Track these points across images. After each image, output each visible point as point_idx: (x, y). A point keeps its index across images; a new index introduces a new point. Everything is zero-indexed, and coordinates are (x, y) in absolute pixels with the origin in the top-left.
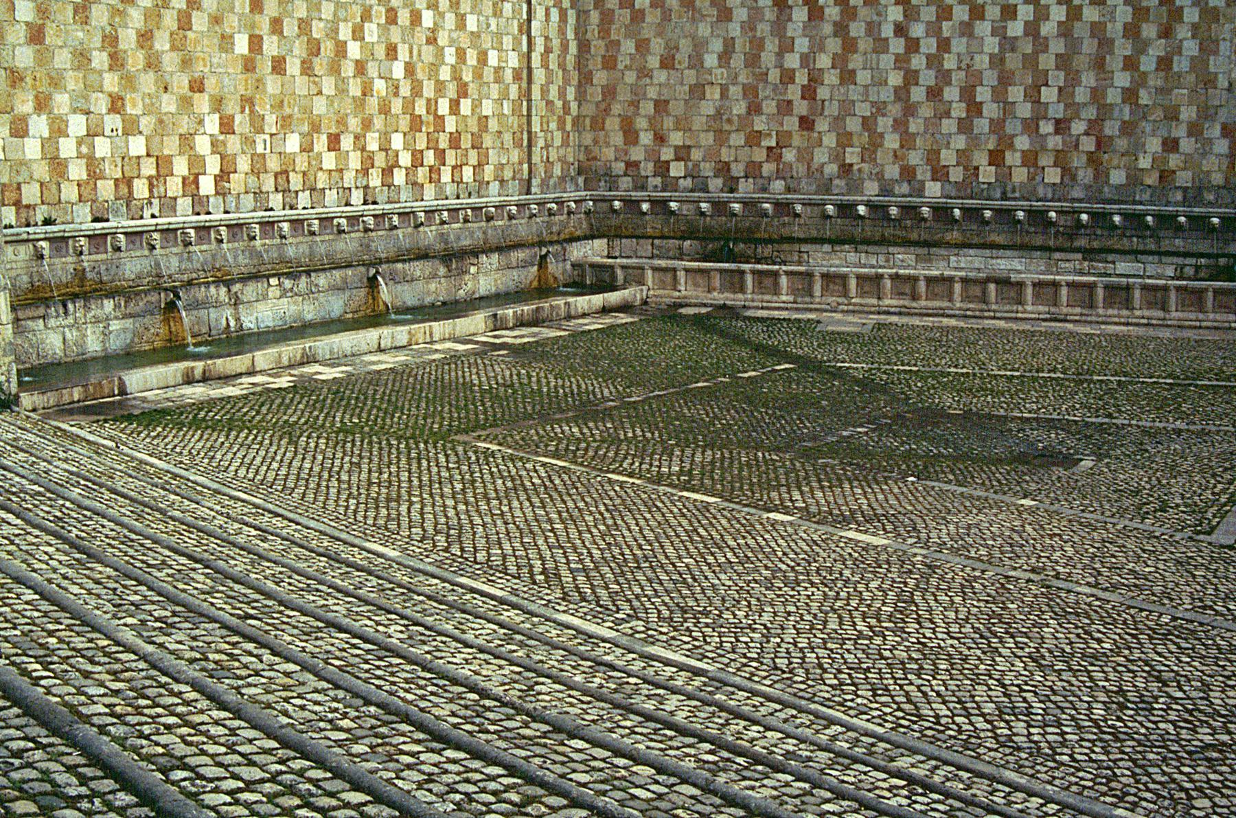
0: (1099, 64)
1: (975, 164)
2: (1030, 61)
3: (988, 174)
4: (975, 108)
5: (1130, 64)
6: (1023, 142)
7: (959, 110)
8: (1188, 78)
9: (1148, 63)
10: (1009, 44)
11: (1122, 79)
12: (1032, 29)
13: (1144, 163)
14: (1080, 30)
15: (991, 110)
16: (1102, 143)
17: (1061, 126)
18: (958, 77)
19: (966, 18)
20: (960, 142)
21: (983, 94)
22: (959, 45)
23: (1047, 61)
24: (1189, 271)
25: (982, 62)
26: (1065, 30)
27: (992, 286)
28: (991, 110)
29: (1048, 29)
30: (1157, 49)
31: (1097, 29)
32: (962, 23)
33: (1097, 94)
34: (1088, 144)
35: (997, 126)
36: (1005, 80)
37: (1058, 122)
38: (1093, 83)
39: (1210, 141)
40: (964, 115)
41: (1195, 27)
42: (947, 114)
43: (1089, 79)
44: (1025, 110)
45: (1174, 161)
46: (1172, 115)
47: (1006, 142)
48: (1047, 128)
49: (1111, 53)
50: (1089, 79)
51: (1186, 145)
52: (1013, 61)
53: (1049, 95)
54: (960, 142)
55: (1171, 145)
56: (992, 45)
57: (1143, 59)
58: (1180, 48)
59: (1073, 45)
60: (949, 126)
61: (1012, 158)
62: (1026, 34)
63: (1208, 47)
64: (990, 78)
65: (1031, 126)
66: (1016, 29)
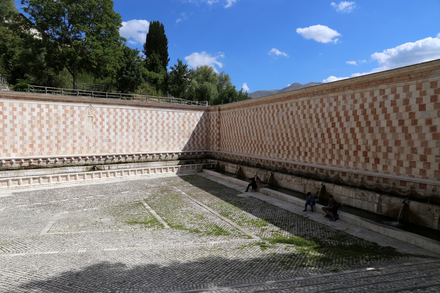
0: (57, 123)
1: (25, 148)
2: (39, 122)
3: (29, 150)
4: (25, 134)
5: (64, 123)
6: (38, 142)
7: (20, 134)
8: (78, 126)
9: (68, 123)
10: (33, 118)
11: (63, 126)
12: (39, 114)
13: (69, 145)
14: (52, 115)
15: (29, 134)
16: (59, 141)
17: (48, 138)
18: (19, 126)
19: (21, 111)
20: (21, 142)
21: (27, 130)
22: (19, 117)
23: (43, 122)
24: (85, 170)
25: (26, 122)
26: (48, 115)
27: (41, 179)
28: (29, 134)
29: (43, 114)
30: (71, 119)
31: (56, 115)
32: (20, 112)
33: (57, 130)
34: (55, 142)
35: (31, 138)
36: (33, 126)
37: (47, 137)
38: (56, 127)
39: (83, 140)
40: (21, 136)
41: (79, 115)
42: (16, 135)
43: (54, 126)
44: (38, 134)
45: (76, 145)
46: (75, 134)
47: (34, 142)
48: (44, 138)
49: (60, 120)
50: (54, 126)
51: (79, 141)
52: (35, 122)
53: (44, 130)
54: (21, 142)
55: (75, 141)
56: (29, 118)
57: (67, 122)
58: (75, 119)
59: (50, 118)
60: (17, 138)
61: (36, 146)
62: (38, 115)
63: (82, 119)
64: (29, 126)
65: (40, 138)
66: (35, 114)
